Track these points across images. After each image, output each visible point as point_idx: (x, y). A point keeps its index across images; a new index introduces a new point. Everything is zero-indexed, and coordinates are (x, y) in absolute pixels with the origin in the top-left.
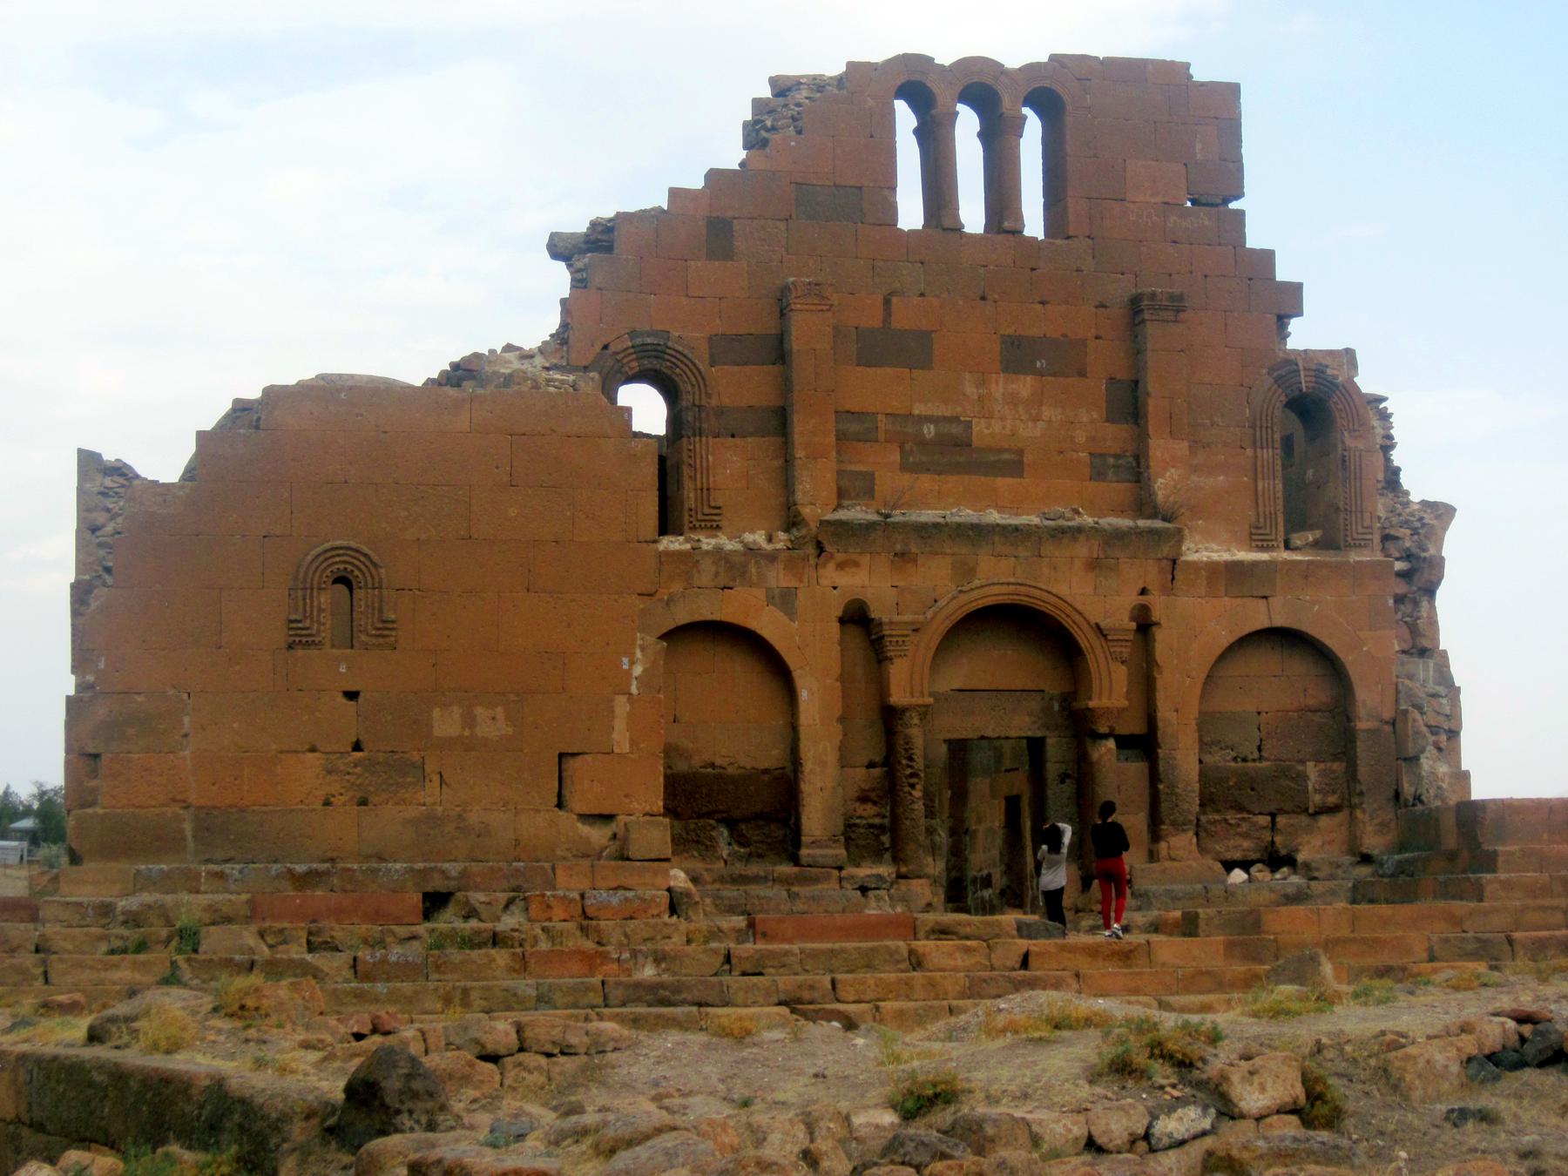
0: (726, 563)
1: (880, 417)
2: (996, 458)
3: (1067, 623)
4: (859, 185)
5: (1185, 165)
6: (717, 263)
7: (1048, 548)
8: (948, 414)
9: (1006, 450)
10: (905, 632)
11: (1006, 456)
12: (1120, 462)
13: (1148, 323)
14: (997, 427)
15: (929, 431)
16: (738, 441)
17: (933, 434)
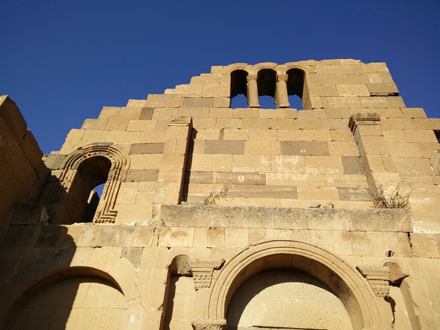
0: (101, 232)
1: (214, 173)
2: (281, 190)
3: (333, 268)
4: (212, 97)
5: (366, 85)
6: (143, 121)
7: (313, 224)
8: (252, 172)
9: (285, 187)
10: (208, 269)
11: (286, 189)
12: (357, 191)
13: (358, 126)
14: (280, 176)
15: (241, 179)
16: (135, 183)
17: (243, 180)
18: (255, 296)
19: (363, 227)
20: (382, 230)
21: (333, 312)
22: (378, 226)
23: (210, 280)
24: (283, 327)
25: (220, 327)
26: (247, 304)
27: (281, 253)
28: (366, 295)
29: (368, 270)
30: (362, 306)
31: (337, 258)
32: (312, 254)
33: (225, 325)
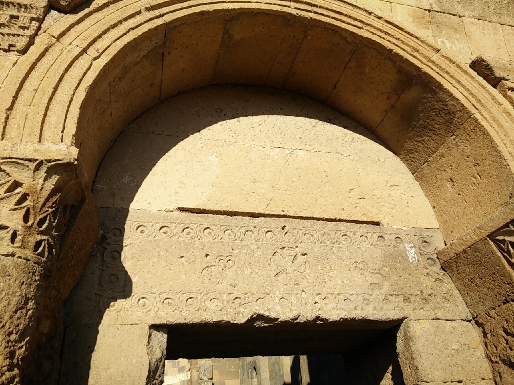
18: (188, 136)
19: (456, 6)
20: (494, 18)
21: (389, 185)
22: (486, 9)
23: (30, 32)
24: (267, 212)
25: (49, 173)
26: (164, 154)
27: (279, 10)
28: (507, 124)
29: (504, 68)
30: (504, 146)
31: (422, 41)
32: (359, 24)
33: (69, 165)
